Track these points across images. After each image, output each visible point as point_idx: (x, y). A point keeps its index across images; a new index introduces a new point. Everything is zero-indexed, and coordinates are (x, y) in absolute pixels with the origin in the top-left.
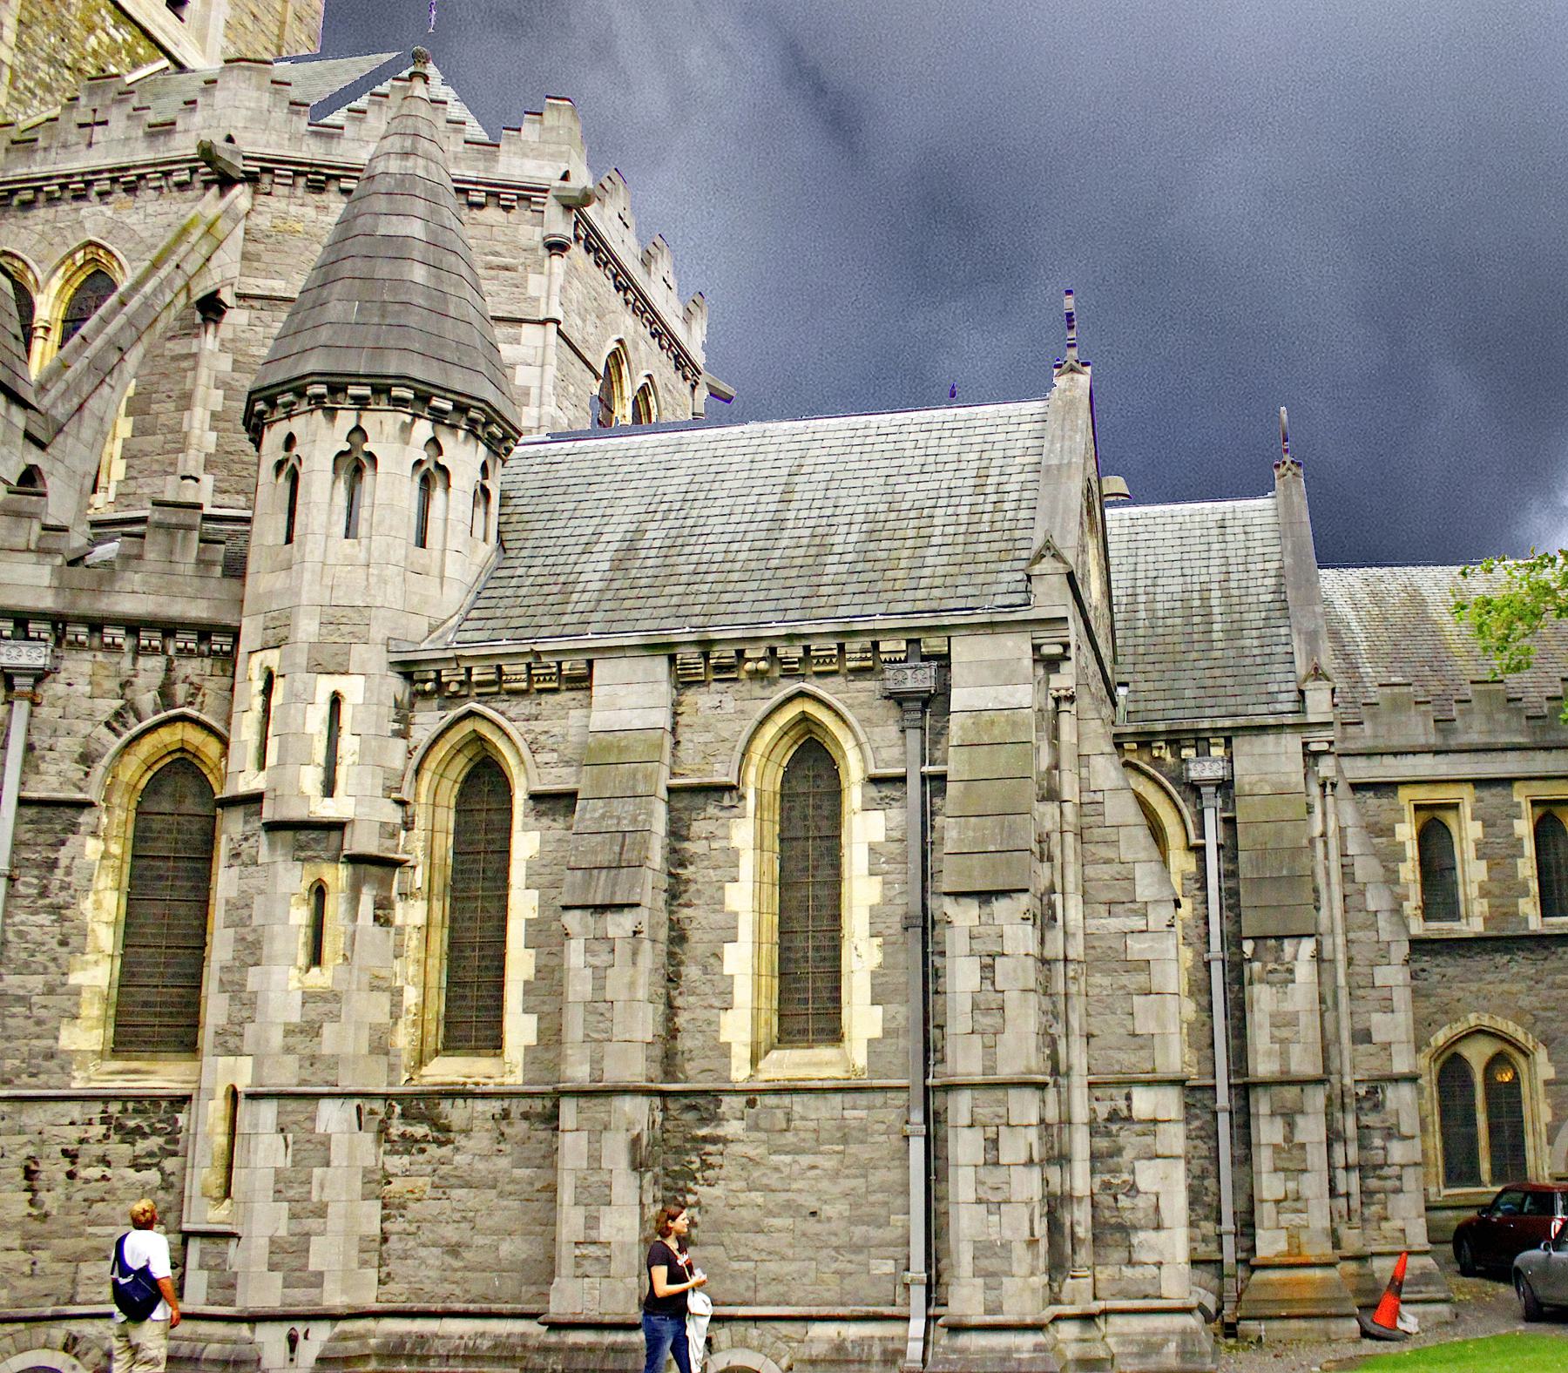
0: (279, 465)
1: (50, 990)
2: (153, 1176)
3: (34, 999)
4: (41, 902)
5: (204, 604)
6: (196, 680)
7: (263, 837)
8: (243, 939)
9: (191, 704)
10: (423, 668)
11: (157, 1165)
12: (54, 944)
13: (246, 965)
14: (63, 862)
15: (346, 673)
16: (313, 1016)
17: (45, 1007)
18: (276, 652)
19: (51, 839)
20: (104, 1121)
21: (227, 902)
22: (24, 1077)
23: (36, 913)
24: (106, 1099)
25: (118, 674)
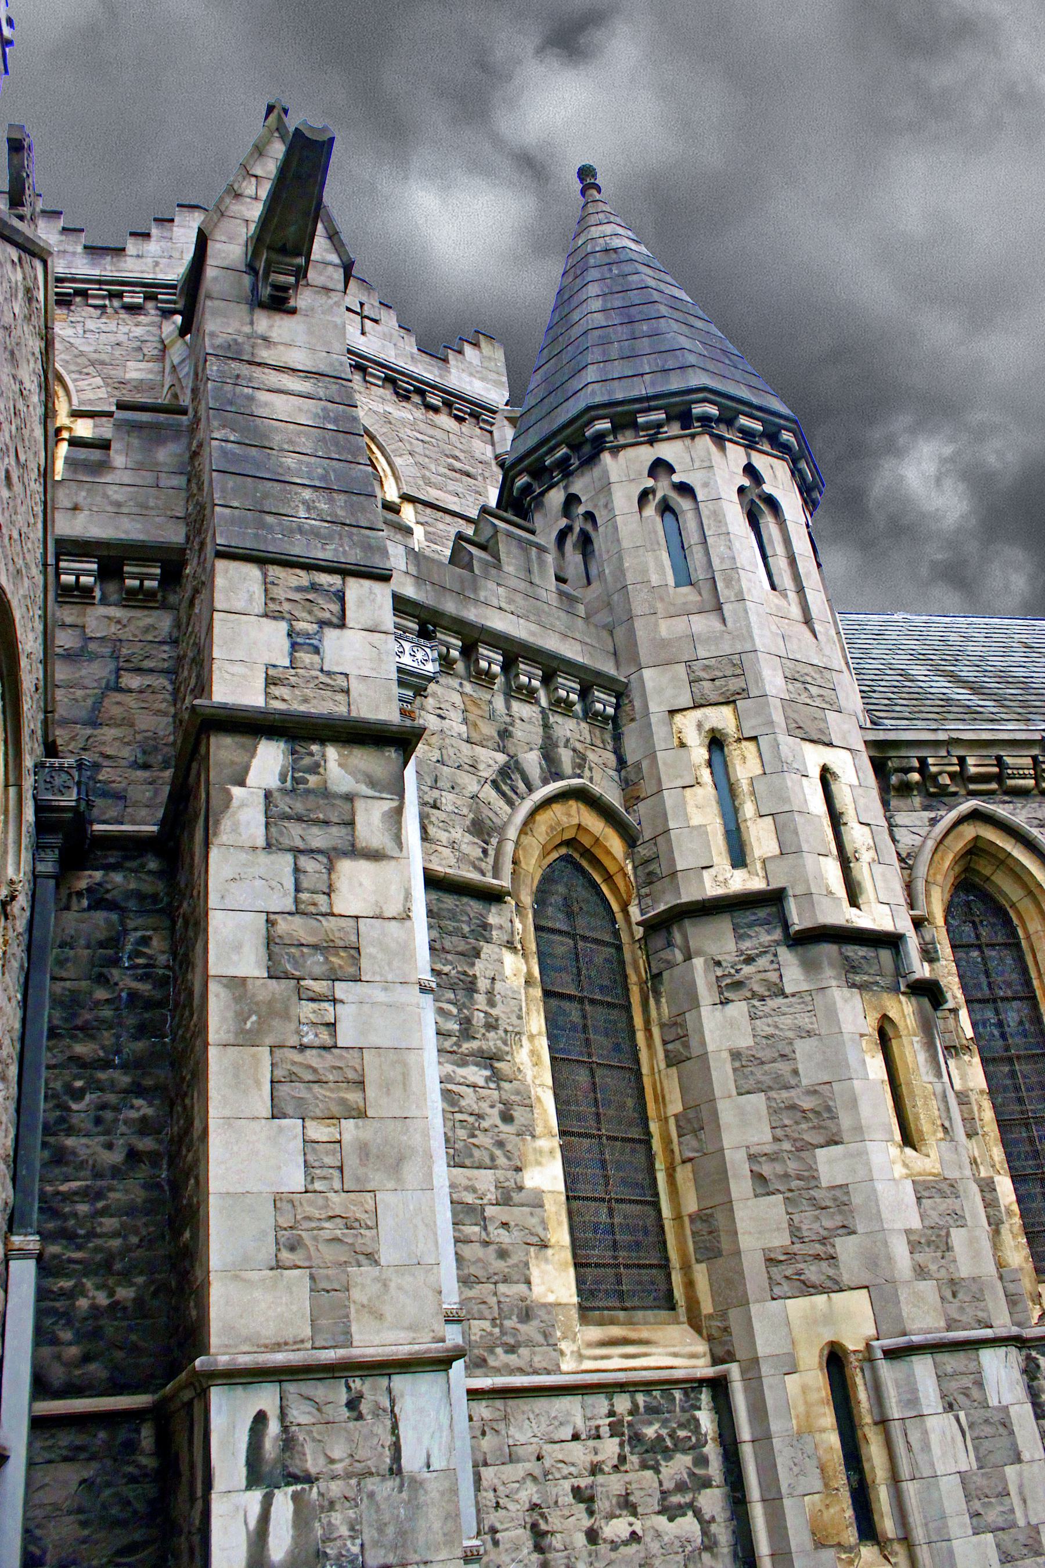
0: (644, 496)
1: (505, 1200)
2: (688, 1525)
3: (490, 1211)
4: (467, 1046)
5: (578, 647)
6: (579, 746)
7: (785, 955)
8: (793, 1107)
9: (580, 776)
10: (903, 753)
11: (691, 1505)
12: (493, 1117)
13: (803, 1148)
14: (483, 984)
15: (830, 745)
16: (934, 1218)
17: (505, 1225)
18: (727, 711)
19: (462, 946)
20: (615, 1430)
21: (735, 1055)
22: (499, 1350)
23: (463, 1064)
24: (609, 1389)
25: (492, 717)
